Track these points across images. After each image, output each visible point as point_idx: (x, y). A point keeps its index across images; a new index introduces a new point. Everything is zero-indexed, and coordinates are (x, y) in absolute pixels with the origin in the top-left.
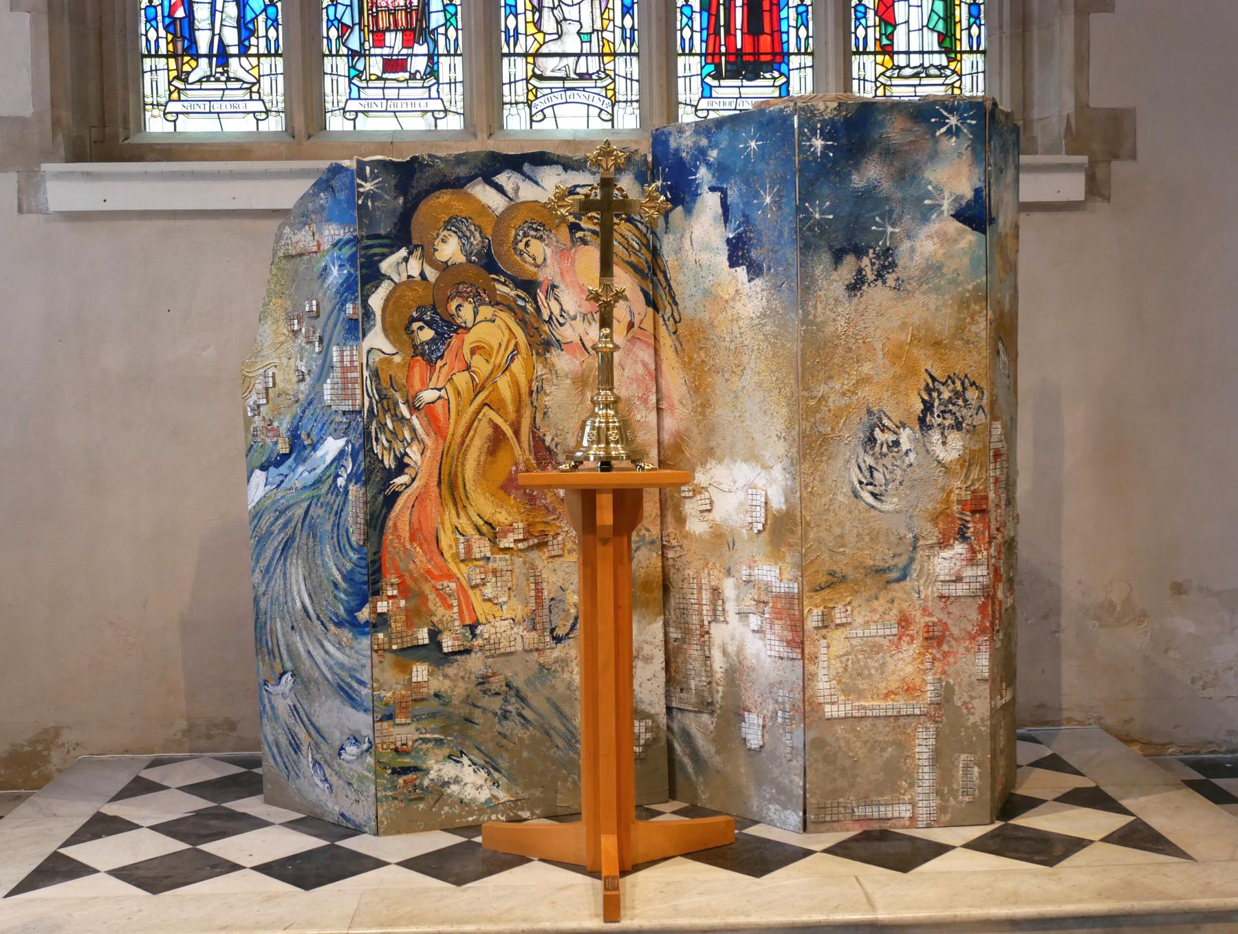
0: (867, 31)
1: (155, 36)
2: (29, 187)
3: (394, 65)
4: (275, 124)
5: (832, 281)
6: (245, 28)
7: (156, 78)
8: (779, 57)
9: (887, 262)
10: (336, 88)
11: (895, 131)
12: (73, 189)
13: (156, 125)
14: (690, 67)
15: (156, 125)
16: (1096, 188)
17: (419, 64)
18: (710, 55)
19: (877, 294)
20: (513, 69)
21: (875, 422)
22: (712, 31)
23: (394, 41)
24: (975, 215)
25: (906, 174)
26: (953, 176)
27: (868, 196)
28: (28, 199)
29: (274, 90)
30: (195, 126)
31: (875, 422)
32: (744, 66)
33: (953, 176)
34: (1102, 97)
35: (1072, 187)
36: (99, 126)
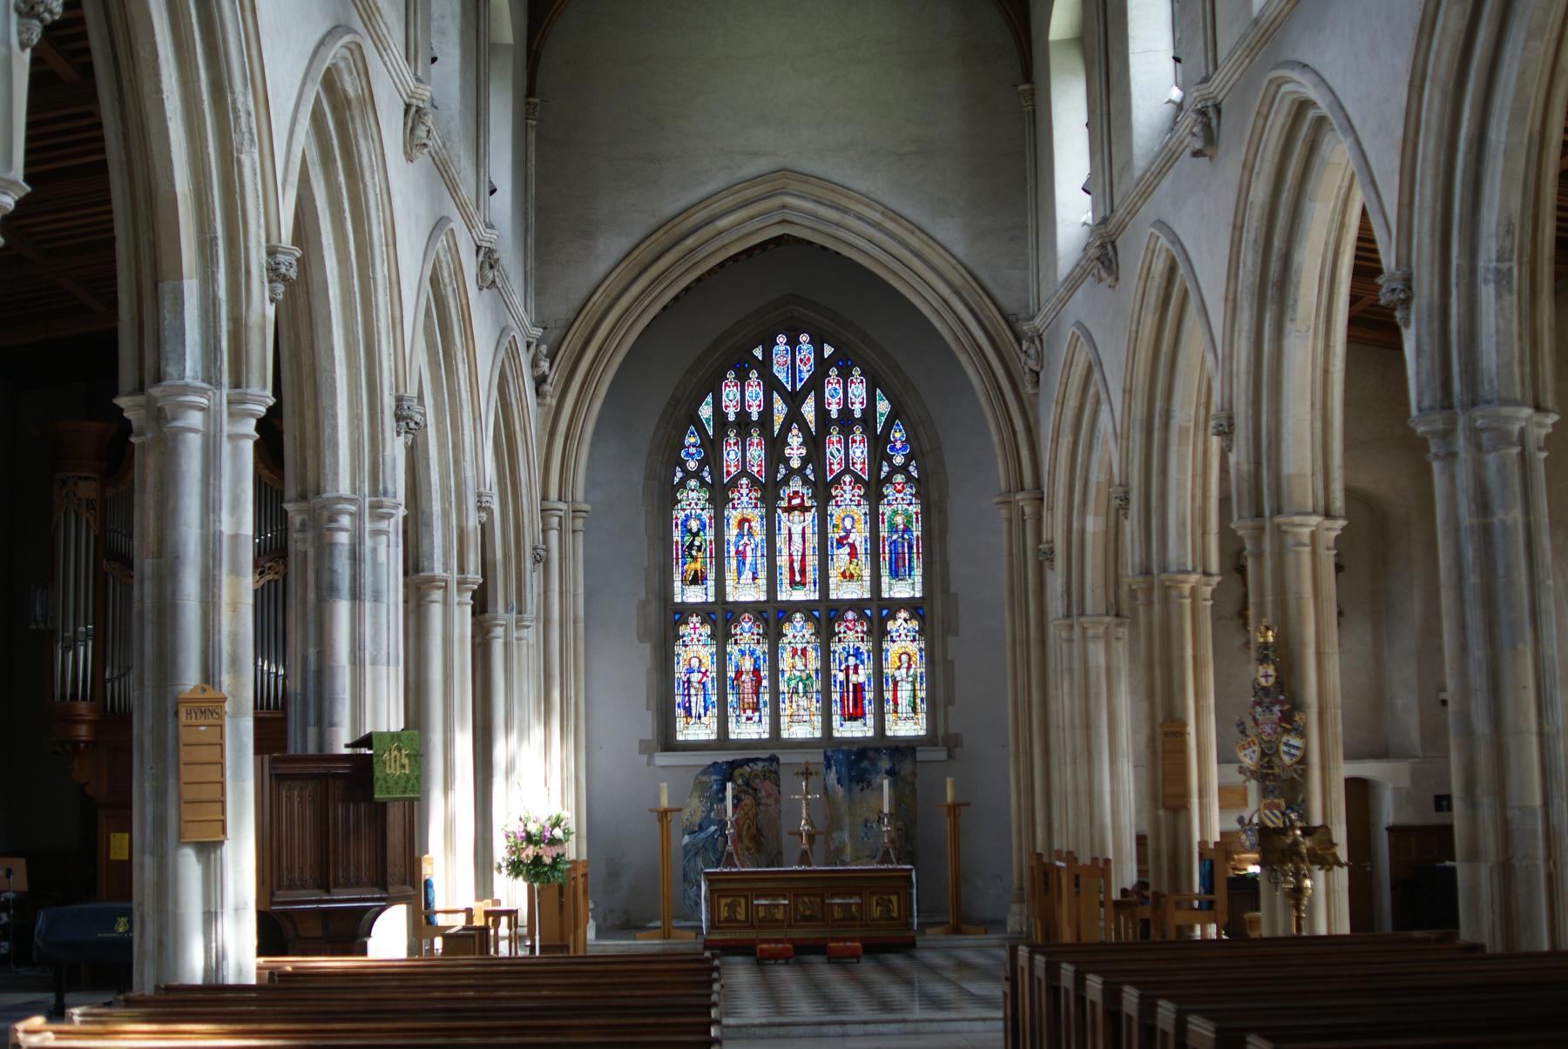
0: (889, 707)
1: (680, 712)
2: (651, 757)
3: (749, 719)
4: (713, 737)
5: (857, 789)
6: (706, 709)
7: (680, 723)
8: (863, 715)
9: (869, 784)
10: (732, 726)
11: (871, 754)
12: (663, 759)
13: (680, 737)
14: (836, 719)
15: (680, 737)
16: (950, 756)
17: (756, 718)
18: (843, 715)
19: (867, 792)
20: (784, 720)
21: (867, 821)
22: (843, 707)
23: (749, 713)
24: (891, 773)
25: (874, 764)
26: (885, 764)
27: (865, 770)
28: (650, 762)
29: (715, 726)
30: (691, 738)
31: (867, 821)
32: (853, 717)
33: (885, 764)
34: (952, 730)
35: (942, 755)
36: (667, 741)
